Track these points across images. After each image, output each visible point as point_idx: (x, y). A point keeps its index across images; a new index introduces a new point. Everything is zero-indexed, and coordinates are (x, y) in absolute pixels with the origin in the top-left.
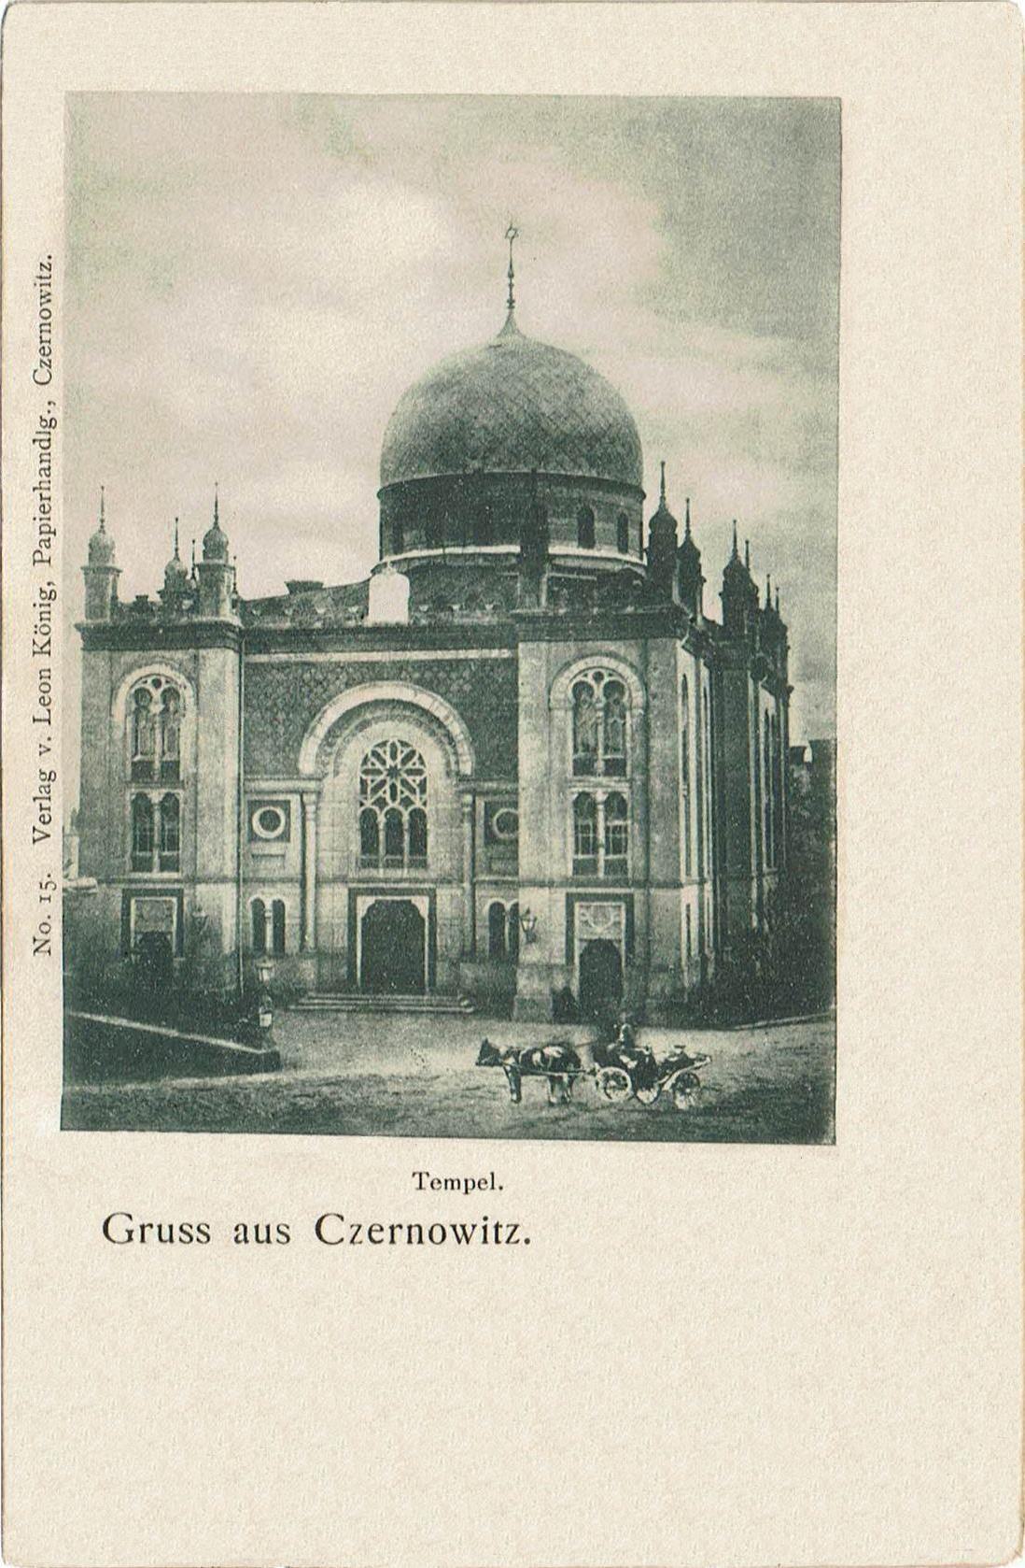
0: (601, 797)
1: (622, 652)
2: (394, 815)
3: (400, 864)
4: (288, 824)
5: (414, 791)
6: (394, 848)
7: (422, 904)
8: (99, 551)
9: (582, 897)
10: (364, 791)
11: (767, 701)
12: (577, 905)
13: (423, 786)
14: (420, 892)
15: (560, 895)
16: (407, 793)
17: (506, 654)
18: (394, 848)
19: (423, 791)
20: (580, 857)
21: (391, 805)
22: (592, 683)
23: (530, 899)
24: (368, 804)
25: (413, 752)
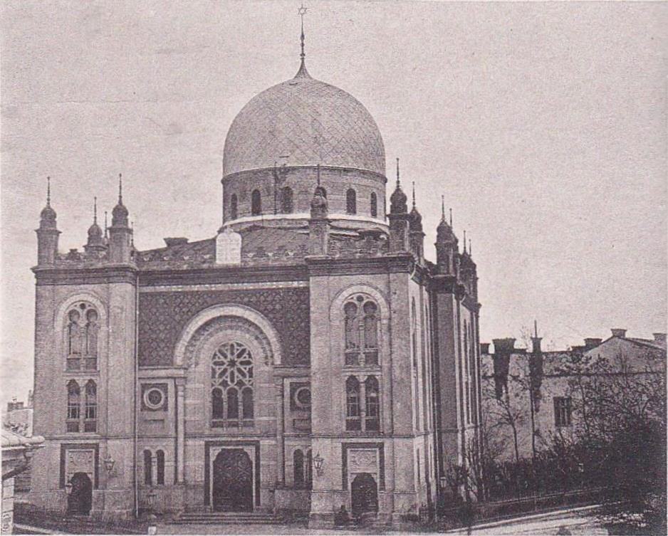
0: (362, 378)
1: (374, 282)
2: (232, 393)
4: (155, 386)
5: (244, 375)
6: (233, 412)
7: (250, 451)
8: (48, 216)
9: (353, 445)
10: (213, 377)
11: (465, 313)
12: (349, 450)
13: (250, 371)
14: (248, 443)
15: (338, 445)
16: (241, 377)
17: (302, 284)
20: (350, 418)
22: (356, 302)
23: (318, 446)
24: (217, 386)
25: (232, 345)
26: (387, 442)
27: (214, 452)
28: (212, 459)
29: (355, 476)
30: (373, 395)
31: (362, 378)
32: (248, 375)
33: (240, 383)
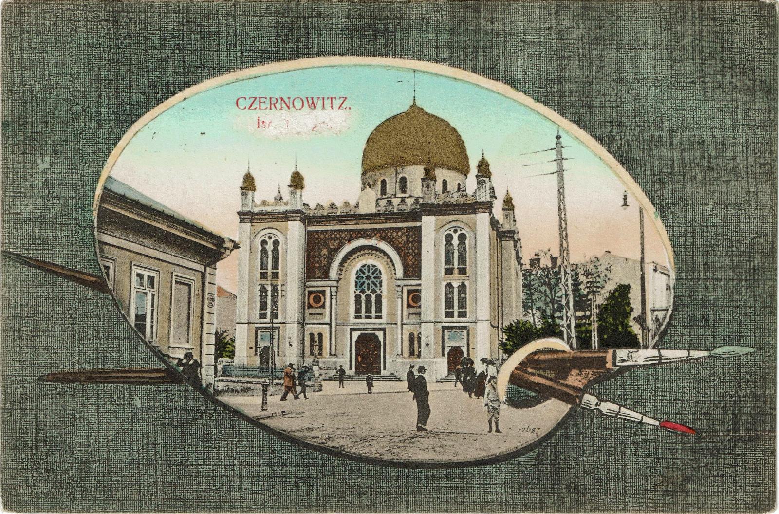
0: (456, 284)
2: (368, 297)
3: (370, 317)
5: (376, 285)
6: (368, 310)
7: (380, 334)
10: (356, 286)
13: (381, 283)
16: (374, 287)
18: (368, 310)
19: (381, 286)
21: (368, 292)
24: (358, 292)
26: (472, 325)
27: (356, 335)
28: (355, 339)
29: (450, 348)
30: (463, 295)
31: (456, 284)
32: (378, 285)
33: (374, 291)
